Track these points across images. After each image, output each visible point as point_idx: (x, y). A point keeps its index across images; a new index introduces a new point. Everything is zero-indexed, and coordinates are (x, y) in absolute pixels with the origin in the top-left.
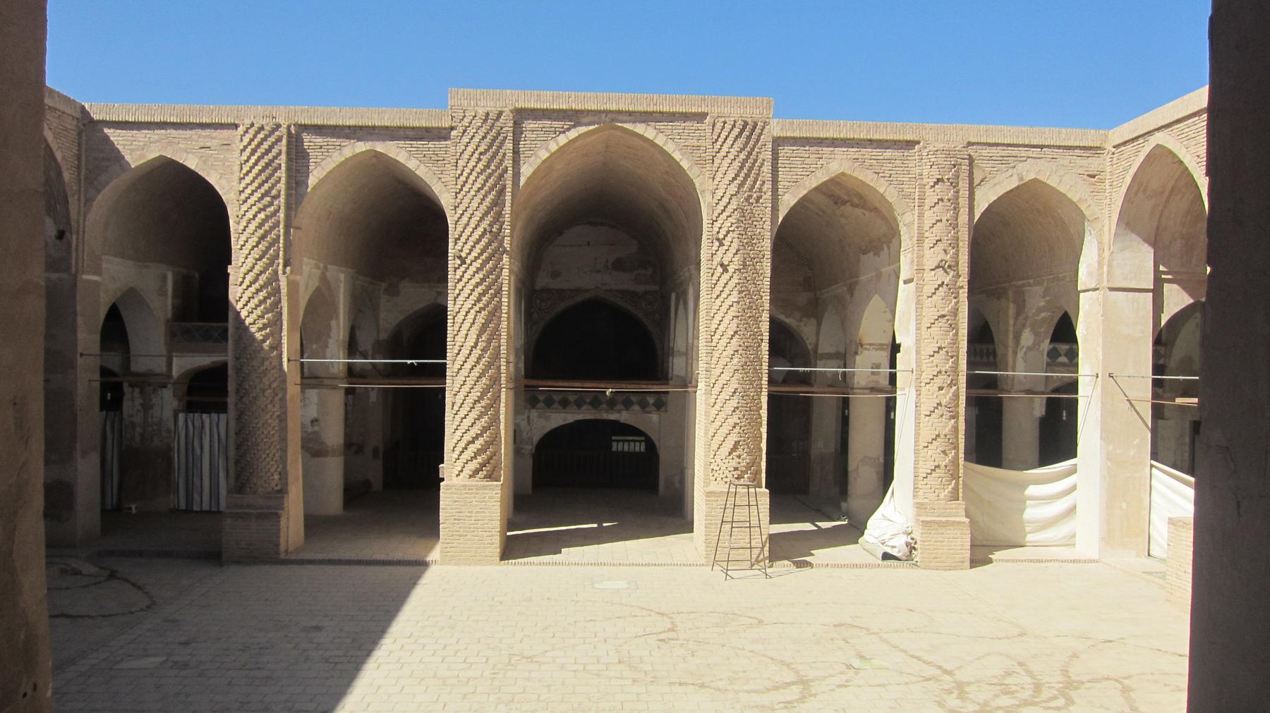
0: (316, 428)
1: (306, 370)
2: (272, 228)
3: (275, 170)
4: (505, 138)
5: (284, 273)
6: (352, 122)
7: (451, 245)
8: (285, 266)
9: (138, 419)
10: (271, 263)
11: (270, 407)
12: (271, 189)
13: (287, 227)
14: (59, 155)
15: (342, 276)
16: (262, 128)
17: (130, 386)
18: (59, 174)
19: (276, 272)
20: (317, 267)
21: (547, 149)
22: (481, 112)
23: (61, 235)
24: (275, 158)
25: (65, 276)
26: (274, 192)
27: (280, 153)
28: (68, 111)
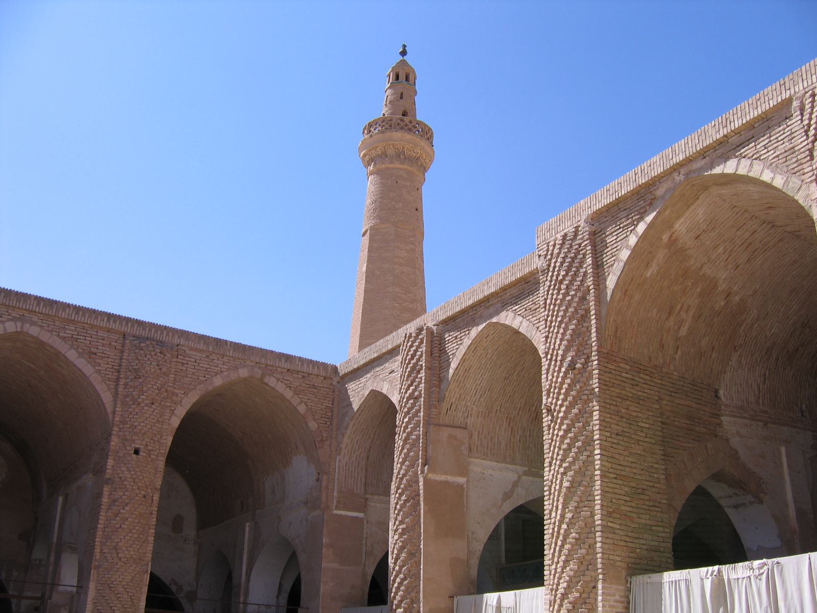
2: (414, 429)
3: (419, 372)
4: (584, 255)
5: (422, 472)
6: (470, 302)
7: (544, 398)
8: (424, 465)
10: (412, 466)
12: (414, 391)
13: (427, 423)
16: (410, 336)
19: (416, 474)
20: (525, 473)
21: (627, 247)
22: (559, 236)
24: (418, 360)
26: (416, 393)
27: (421, 356)
28: (315, 371)
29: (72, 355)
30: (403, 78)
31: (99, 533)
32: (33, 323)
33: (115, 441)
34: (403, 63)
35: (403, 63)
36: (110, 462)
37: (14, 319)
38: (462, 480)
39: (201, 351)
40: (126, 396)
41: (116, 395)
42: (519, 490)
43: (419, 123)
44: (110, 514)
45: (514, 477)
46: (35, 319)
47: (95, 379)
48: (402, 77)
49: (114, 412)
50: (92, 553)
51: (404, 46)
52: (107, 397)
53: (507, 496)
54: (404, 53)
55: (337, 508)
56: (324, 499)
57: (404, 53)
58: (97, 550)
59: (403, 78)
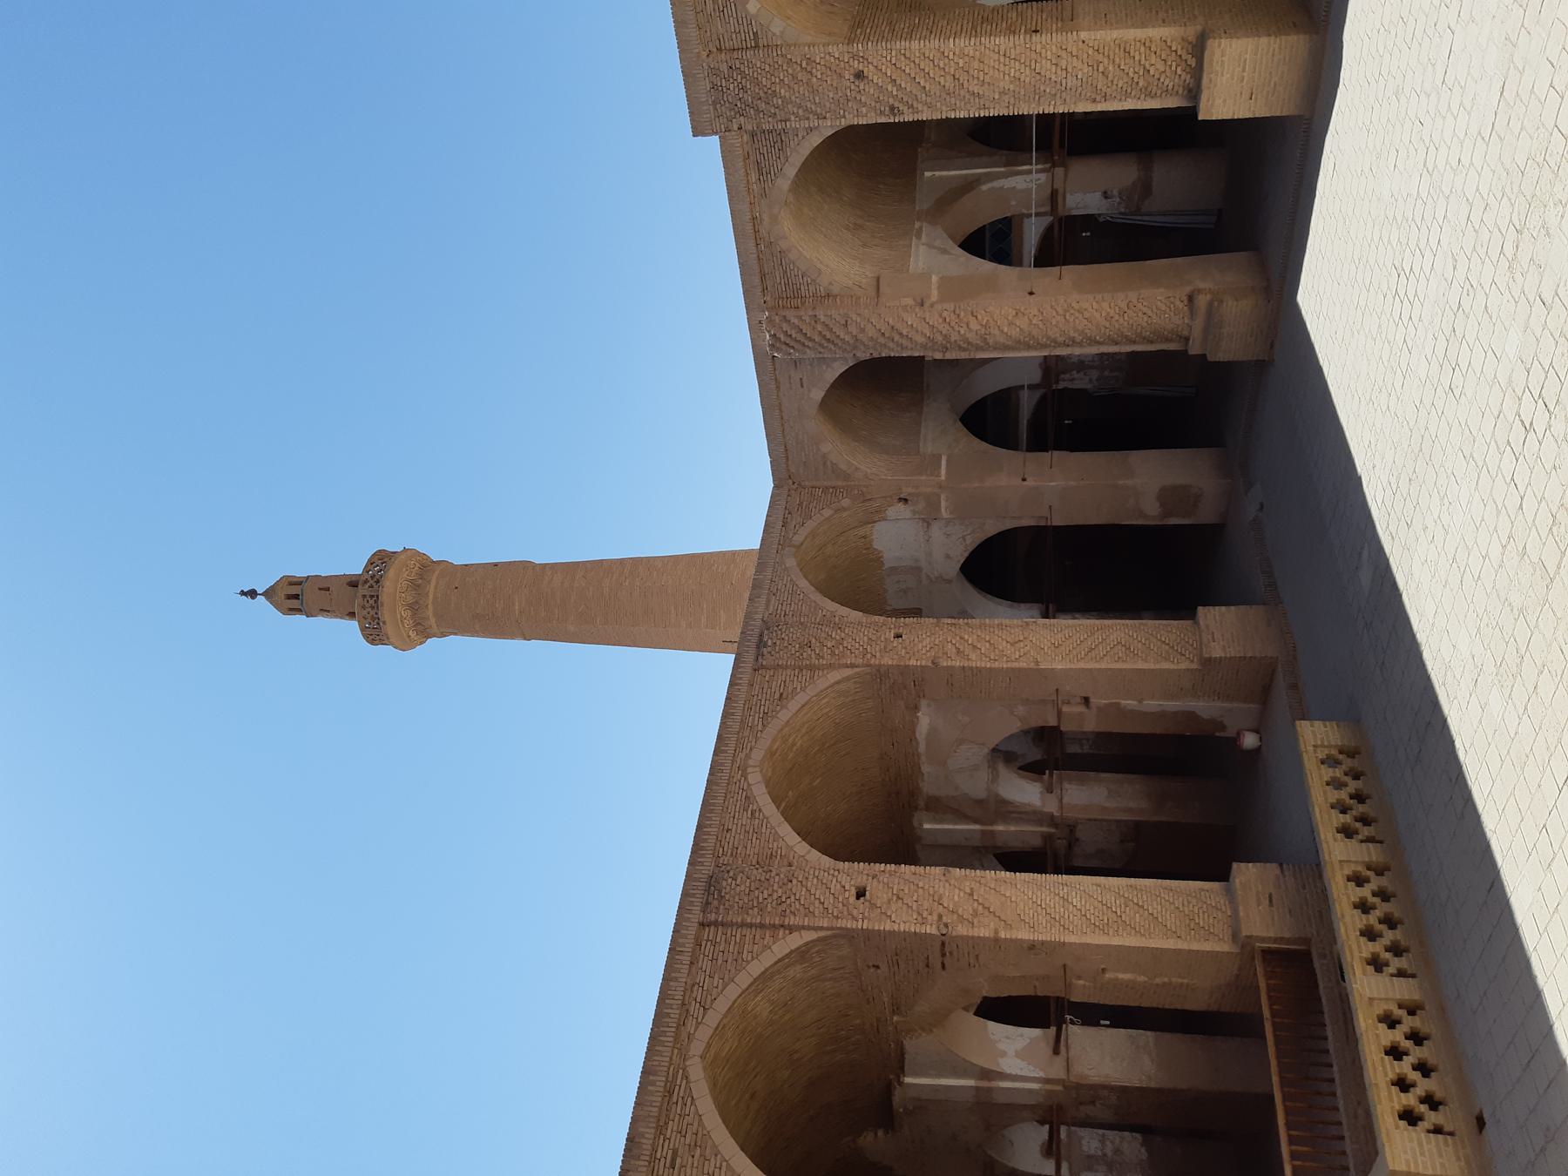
0: (1115, 192)
1: (1042, 210)
9: (1095, 374)
11: (1087, 315)
14: (827, 513)
15: (928, 174)
17: (1057, 382)
18: (844, 509)
20: (919, 236)
23: (906, 500)
25: (943, 497)
27: (800, 318)
29: (784, 715)
30: (295, 596)
31: (996, 665)
32: (748, 756)
33: (887, 661)
34: (268, 594)
35: (268, 594)
36: (913, 662)
37: (745, 776)
38: (934, 278)
39: (768, 601)
40: (833, 654)
41: (831, 667)
42: (937, 243)
43: (366, 570)
44: (973, 657)
45: (922, 249)
46: (742, 755)
47: (811, 691)
48: (294, 590)
49: (852, 666)
50: (1020, 670)
51: (243, 593)
52: (834, 676)
53: (944, 251)
54: (252, 594)
55: (939, 475)
56: (929, 490)
57: (252, 594)
58: (1015, 665)
59: (295, 596)
